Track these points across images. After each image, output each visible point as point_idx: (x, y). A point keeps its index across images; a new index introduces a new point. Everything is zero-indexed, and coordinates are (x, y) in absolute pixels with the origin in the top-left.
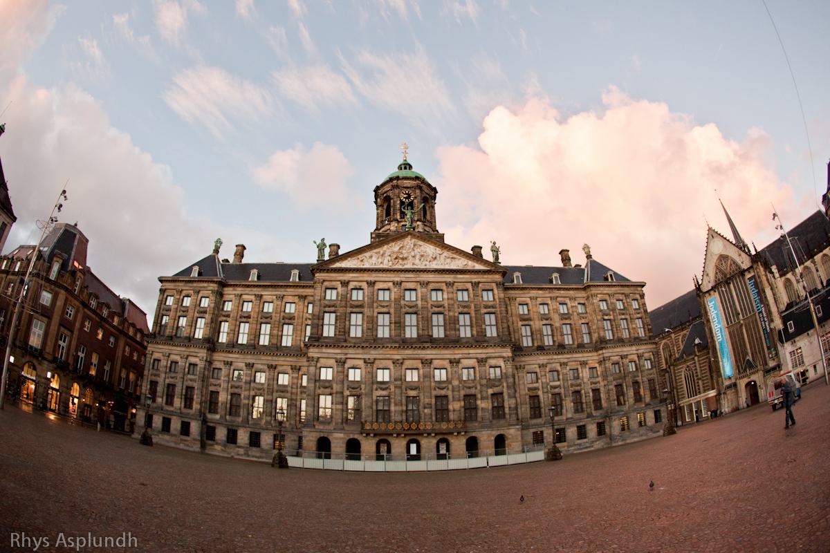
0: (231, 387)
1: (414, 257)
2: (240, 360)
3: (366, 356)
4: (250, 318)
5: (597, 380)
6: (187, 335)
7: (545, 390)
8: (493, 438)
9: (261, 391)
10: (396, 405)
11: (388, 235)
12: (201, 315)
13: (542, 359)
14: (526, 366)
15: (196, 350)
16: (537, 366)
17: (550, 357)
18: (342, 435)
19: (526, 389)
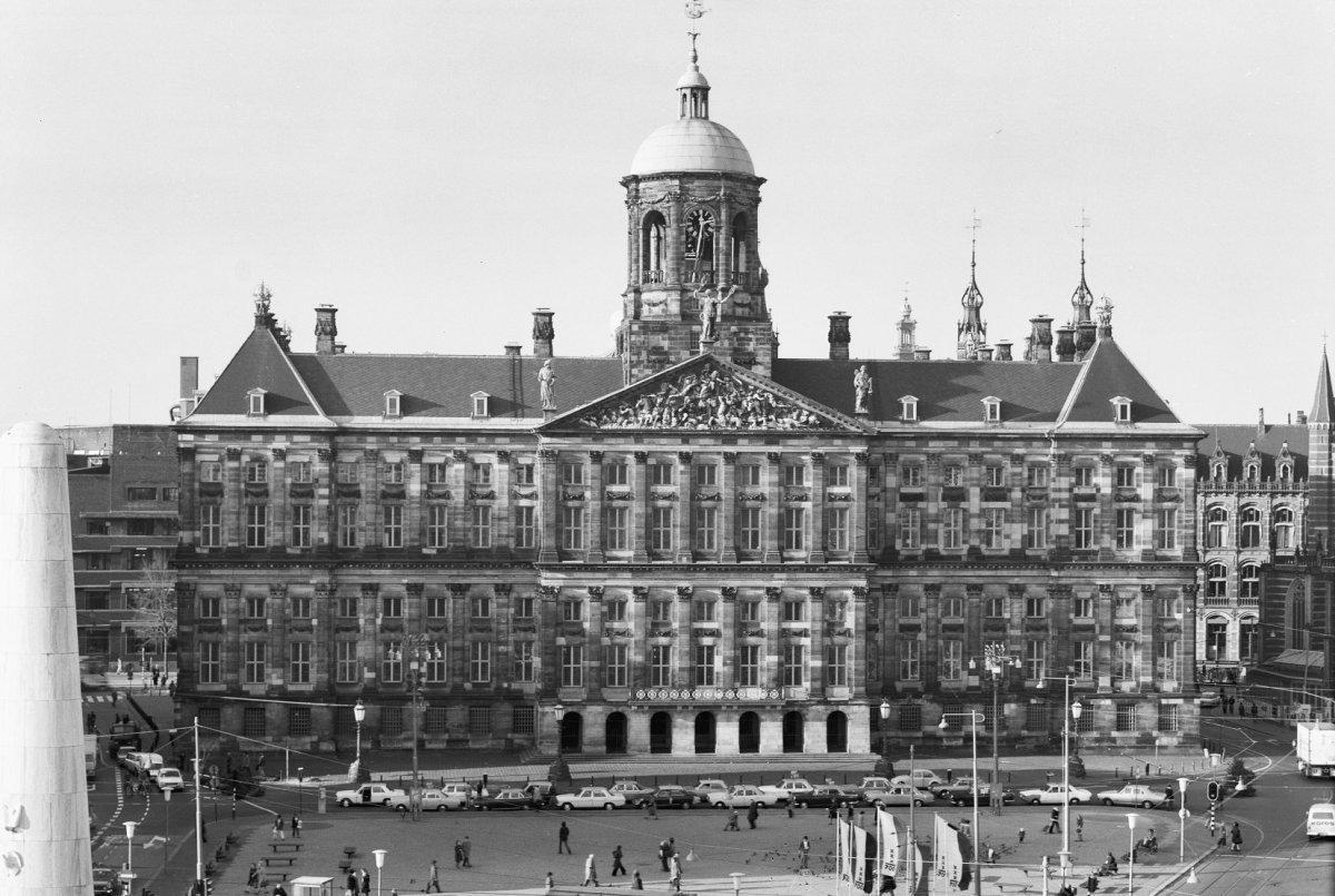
0: (382, 631)
1: (713, 408)
2: (393, 581)
3: (639, 583)
4: (404, 497)
5: (1043, 623)
6: (278, 544)
7: (932, 632)
8: (825, 717)
9: (442, 632)
10: (681, 659)
11: (663, 328)
12: (302, 501)
13: (934, 575)
14: (901, 587)
15: (305, 572)
16: (921, 589)
17: (951, 573)
18: (599, 709)
19: (897, 627)
